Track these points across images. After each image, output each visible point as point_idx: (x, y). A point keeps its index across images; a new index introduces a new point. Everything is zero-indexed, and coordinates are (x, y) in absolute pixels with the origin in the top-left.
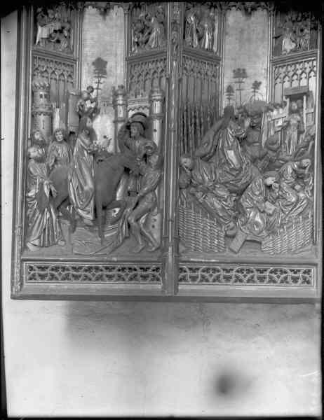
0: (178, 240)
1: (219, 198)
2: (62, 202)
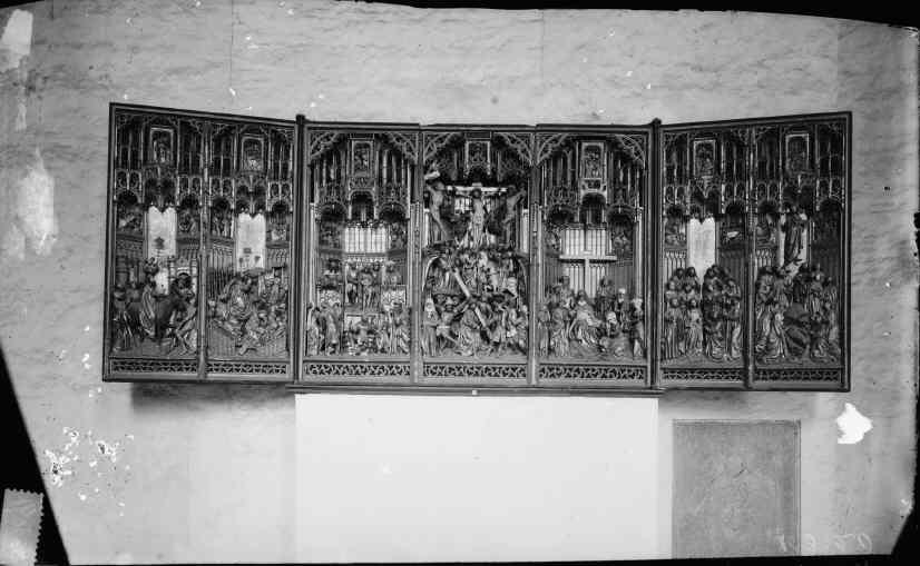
0: (207, 347)
1: (232, 324)
2: (134, 324)
